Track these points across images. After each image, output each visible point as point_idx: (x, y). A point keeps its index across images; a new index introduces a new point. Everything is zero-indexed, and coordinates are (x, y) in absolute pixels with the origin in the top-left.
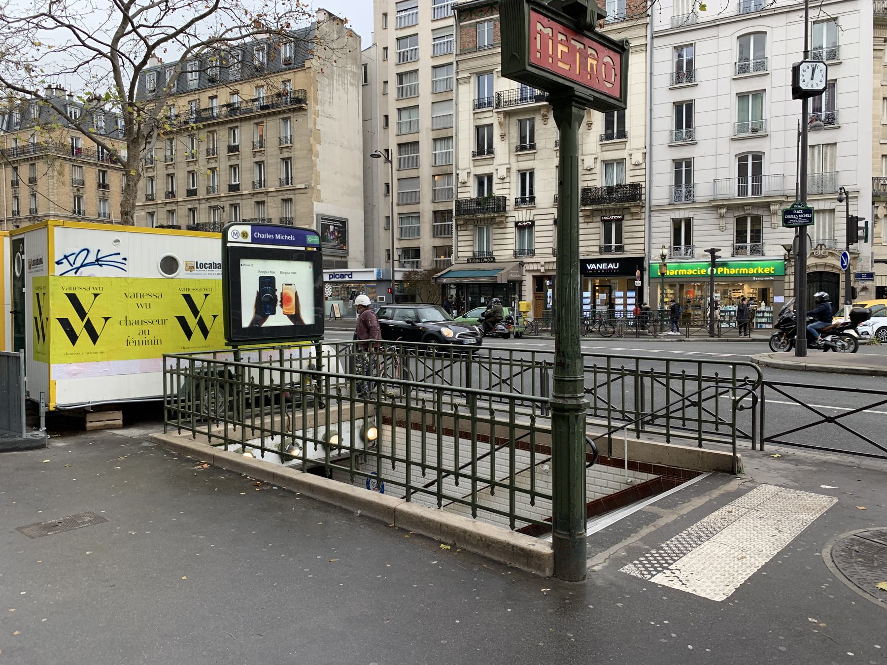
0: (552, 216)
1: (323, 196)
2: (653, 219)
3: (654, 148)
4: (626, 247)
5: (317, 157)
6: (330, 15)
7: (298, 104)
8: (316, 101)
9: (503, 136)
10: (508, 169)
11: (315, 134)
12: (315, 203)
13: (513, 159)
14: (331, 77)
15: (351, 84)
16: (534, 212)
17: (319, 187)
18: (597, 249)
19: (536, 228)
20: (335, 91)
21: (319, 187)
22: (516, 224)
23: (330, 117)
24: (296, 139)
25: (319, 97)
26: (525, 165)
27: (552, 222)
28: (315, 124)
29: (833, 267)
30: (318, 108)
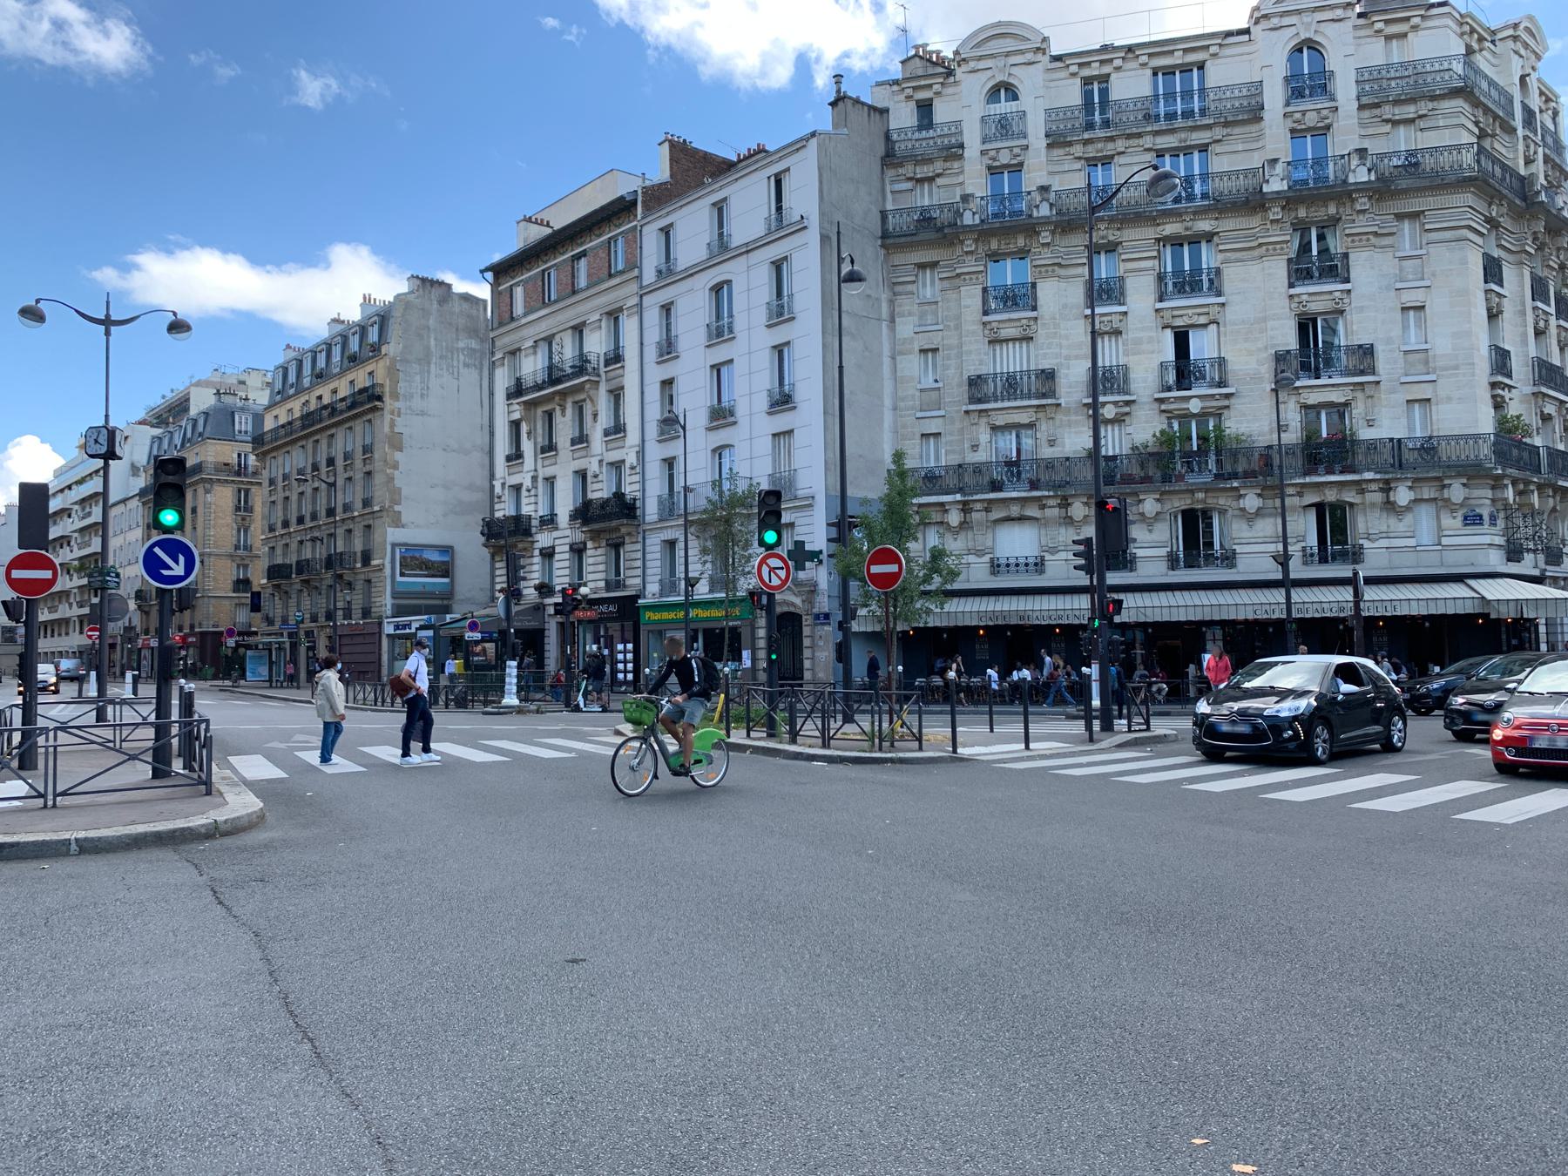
0: (567, 540)
1: (404, 519)
2: (648, 542)
3: (647, 444)
4: (628, 582)
5: (395, 466)
6: (424, 280)
7: (368, 400)
8: (395, 396)
9: (529, 433)
10: (534, 479)
11: (397, 443)
12: (390, 530)
13: (540, 462)
14: (425, 360)
15: (466, 365)
16: (555, 534)
17: (397, 508)
18: (602, 584)
19: (557, 557)
20: (432, 376)
21: (397, 508)
22: (541, 554)
23: (423, 413)
24: (376, 447)
25: (401, 391)
26: (549, 471)
27: (567, 548)
28: (392, 424)
29: (793, 604)
30: (397, 404)
